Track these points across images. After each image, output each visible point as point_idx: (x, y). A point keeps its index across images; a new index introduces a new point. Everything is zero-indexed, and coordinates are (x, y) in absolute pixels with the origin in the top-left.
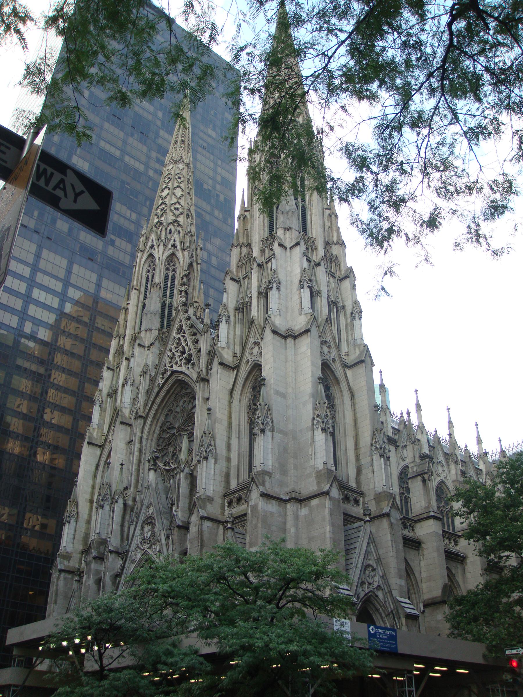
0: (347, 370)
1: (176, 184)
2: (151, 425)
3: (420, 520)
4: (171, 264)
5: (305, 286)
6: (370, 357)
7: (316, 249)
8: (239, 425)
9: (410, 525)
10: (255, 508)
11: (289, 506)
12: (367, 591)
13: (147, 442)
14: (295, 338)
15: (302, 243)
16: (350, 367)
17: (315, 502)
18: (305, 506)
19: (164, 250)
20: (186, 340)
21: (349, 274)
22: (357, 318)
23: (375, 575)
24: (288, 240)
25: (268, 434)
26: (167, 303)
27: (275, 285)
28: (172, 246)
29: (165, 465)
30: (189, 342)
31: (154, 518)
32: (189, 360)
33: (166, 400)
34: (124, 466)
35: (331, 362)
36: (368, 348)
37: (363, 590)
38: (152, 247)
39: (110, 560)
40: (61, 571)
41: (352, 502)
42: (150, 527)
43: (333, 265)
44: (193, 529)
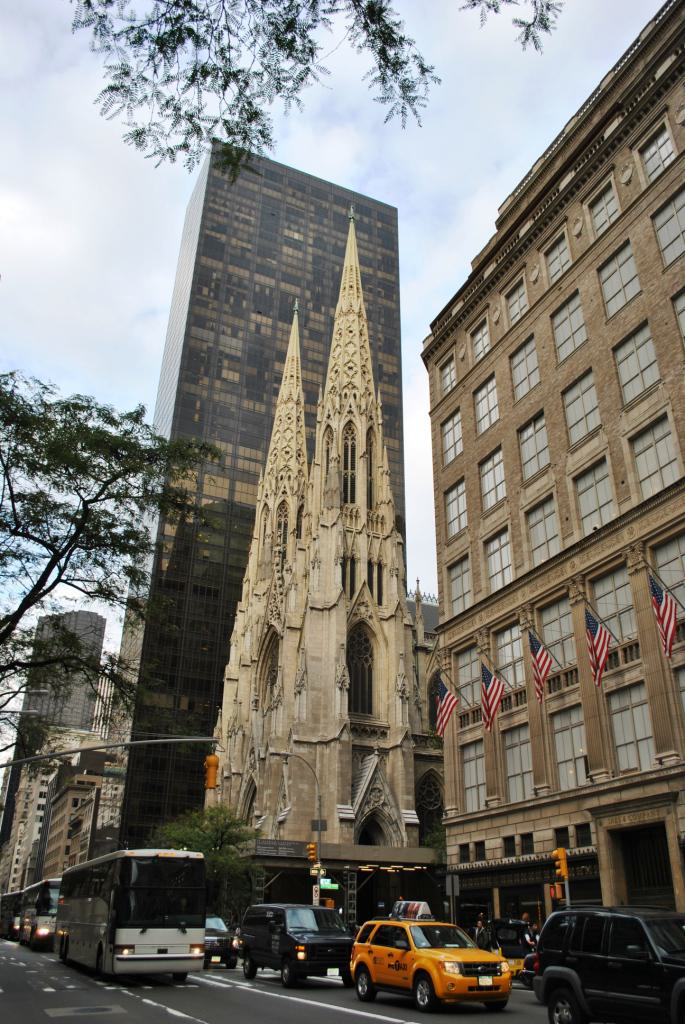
1: (286, 426)
12: (371, 807)
14: (330, 609)
16: (387, 620)
17: (333, 744)
25: (304, 692)
38: (267, 496)
43: (380, 525)
44: (267, 762)
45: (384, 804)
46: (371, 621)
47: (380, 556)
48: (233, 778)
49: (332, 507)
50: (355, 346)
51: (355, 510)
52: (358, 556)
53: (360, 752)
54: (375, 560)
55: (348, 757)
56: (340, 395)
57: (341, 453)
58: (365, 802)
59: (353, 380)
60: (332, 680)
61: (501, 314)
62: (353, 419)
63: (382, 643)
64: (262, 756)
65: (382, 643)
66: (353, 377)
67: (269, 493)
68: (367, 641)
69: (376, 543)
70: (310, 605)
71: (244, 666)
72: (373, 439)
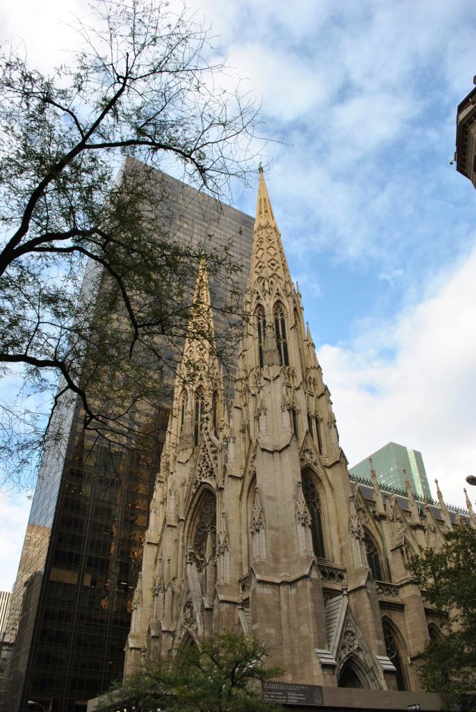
0: (327, 470)
2: (189, 526)
3: (402, 586)
6: (344, 457)
8: (247, 523)
9: (394, 591)
10: (254, 592)
11: (281, 587)
12: (347, 653)
13: (187, 539)
14: (280, 452)
15: (282, 375)
16: (329, 467)
17: (300, 583)
18: (294, 587)
20: (209, 457)
21: (326, 392)
22: (333, 427)
23: (355, 639)
25: (262, 531)
26: (199, 425)
27: (262, 411)
29: (201, 557)
30: (211, 458)
31: (191, 603)
32: (211, 472)
33: (199, 505)
36: (342, 451)
39: (163, 638)
40: (131, 649)
41: (337, 578)
42: (190, 610)
43: (312, 386)
44: (215, 611)
45: (359, 649)
46: (315, 467)
48: (164, 636)
49: (273, 364)
50: (275, 249)
52: (298, 408)
53: (329, 594)
54: (313, 413)
55: (320, 597)
58: (342, 647)
59: (277, 273)
64: (207, 606)
66: (276, 270)
68: (313, 486)
69: (312, 400)
71: (169, 526)
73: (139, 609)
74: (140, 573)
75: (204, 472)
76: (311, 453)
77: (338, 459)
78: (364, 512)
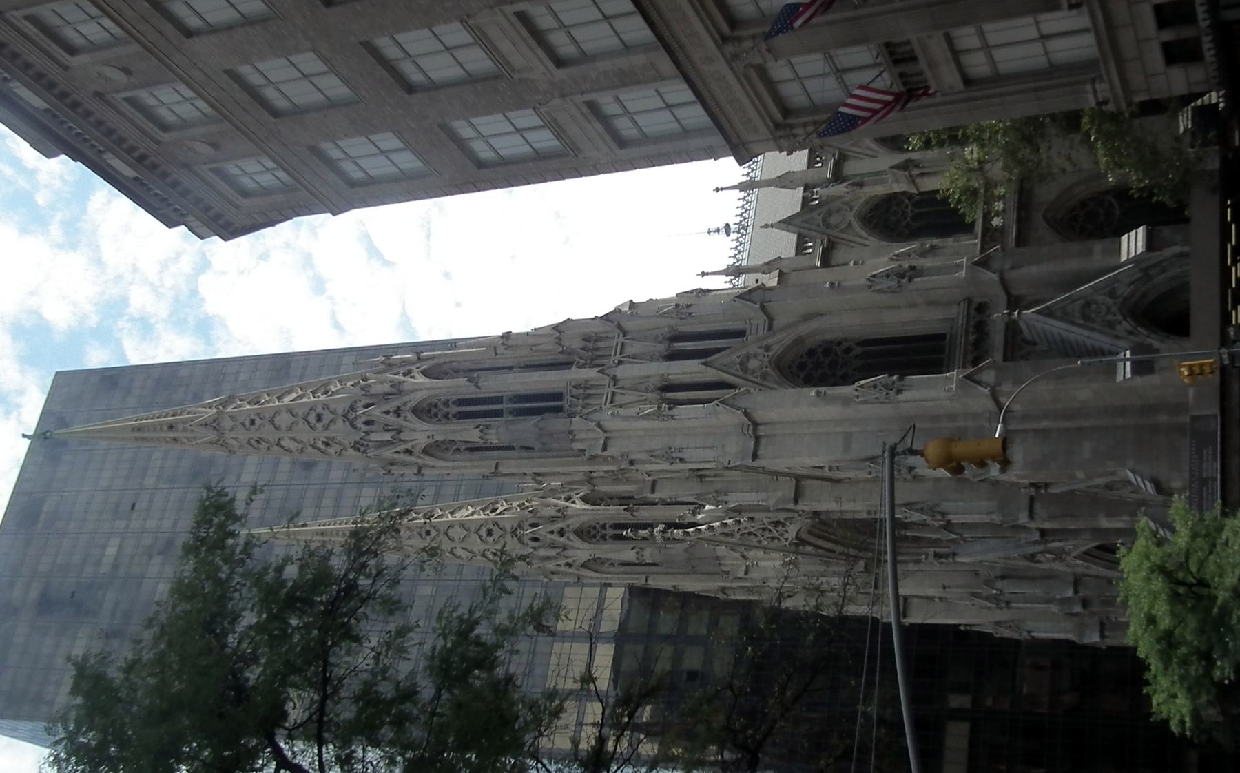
0: (776, 324)
4: (593, 532)
5: (671, 413)
7: (587, 381)
12: (1120, 317)
14: (756, 425)
16: (771, 319)
19: (573, 548)
24: (591, 435)
27: (674, 455)
28: (562, 536)
32: (777, 524)
34: (946, 585)
35: (770, 354)
37: (1120, 323)
38: (569, 565)
40: (1103, 636)
42: (1038, 555)
43: (600, 345)
44: (1047, 525)
45: (1112, 294)
47: (656, 339)
49: (570, 432)
51: (575, 392)
52: (656, 381)
54: (662, 348)
56: (367, 433)
57: (469, 424)
59: (340, 411)
60: (887, 410)
61: (107, 63)
62: (409, 405)
63: (814, 325)
65: (814, 325)
67: (563, 562)
68: (811, 352)
70: (749, 462)
72: (446, 368)
73: (1030, 625)
74: (962, 628)
75: (776, 534)
76: (748, 357)
77: (758, 306)
78: (830, 213)
